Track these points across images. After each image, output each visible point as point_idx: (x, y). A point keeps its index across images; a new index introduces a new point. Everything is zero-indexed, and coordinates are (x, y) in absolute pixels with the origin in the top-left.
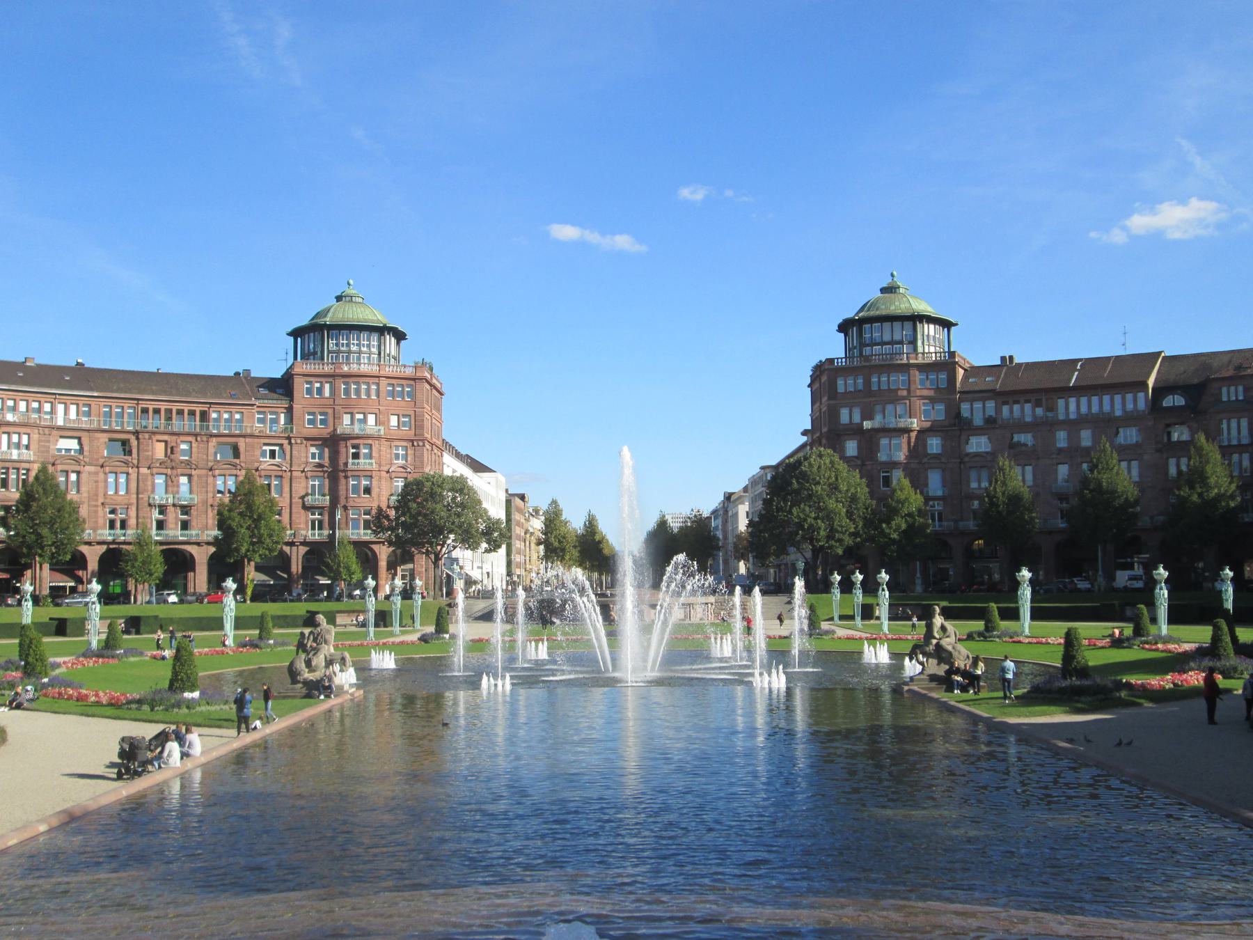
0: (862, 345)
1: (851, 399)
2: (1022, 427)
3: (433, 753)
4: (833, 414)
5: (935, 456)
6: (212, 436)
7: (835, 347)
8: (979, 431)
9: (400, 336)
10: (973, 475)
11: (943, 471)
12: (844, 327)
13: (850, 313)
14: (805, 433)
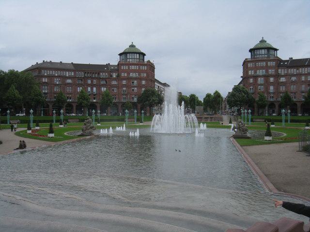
0: (255, 55)
1: (251, 69)
2: (294, 75)
3: (207, 137)
4: (247, 72)
5: (272, 83)
6: (101, 78)
7: (248, 56)
8: (283, 76)
9: (144, 55)
10: (281, 87)
11: (274, 86)
12: (251, 51)
13: (252, 47)
14: (241, 77)
